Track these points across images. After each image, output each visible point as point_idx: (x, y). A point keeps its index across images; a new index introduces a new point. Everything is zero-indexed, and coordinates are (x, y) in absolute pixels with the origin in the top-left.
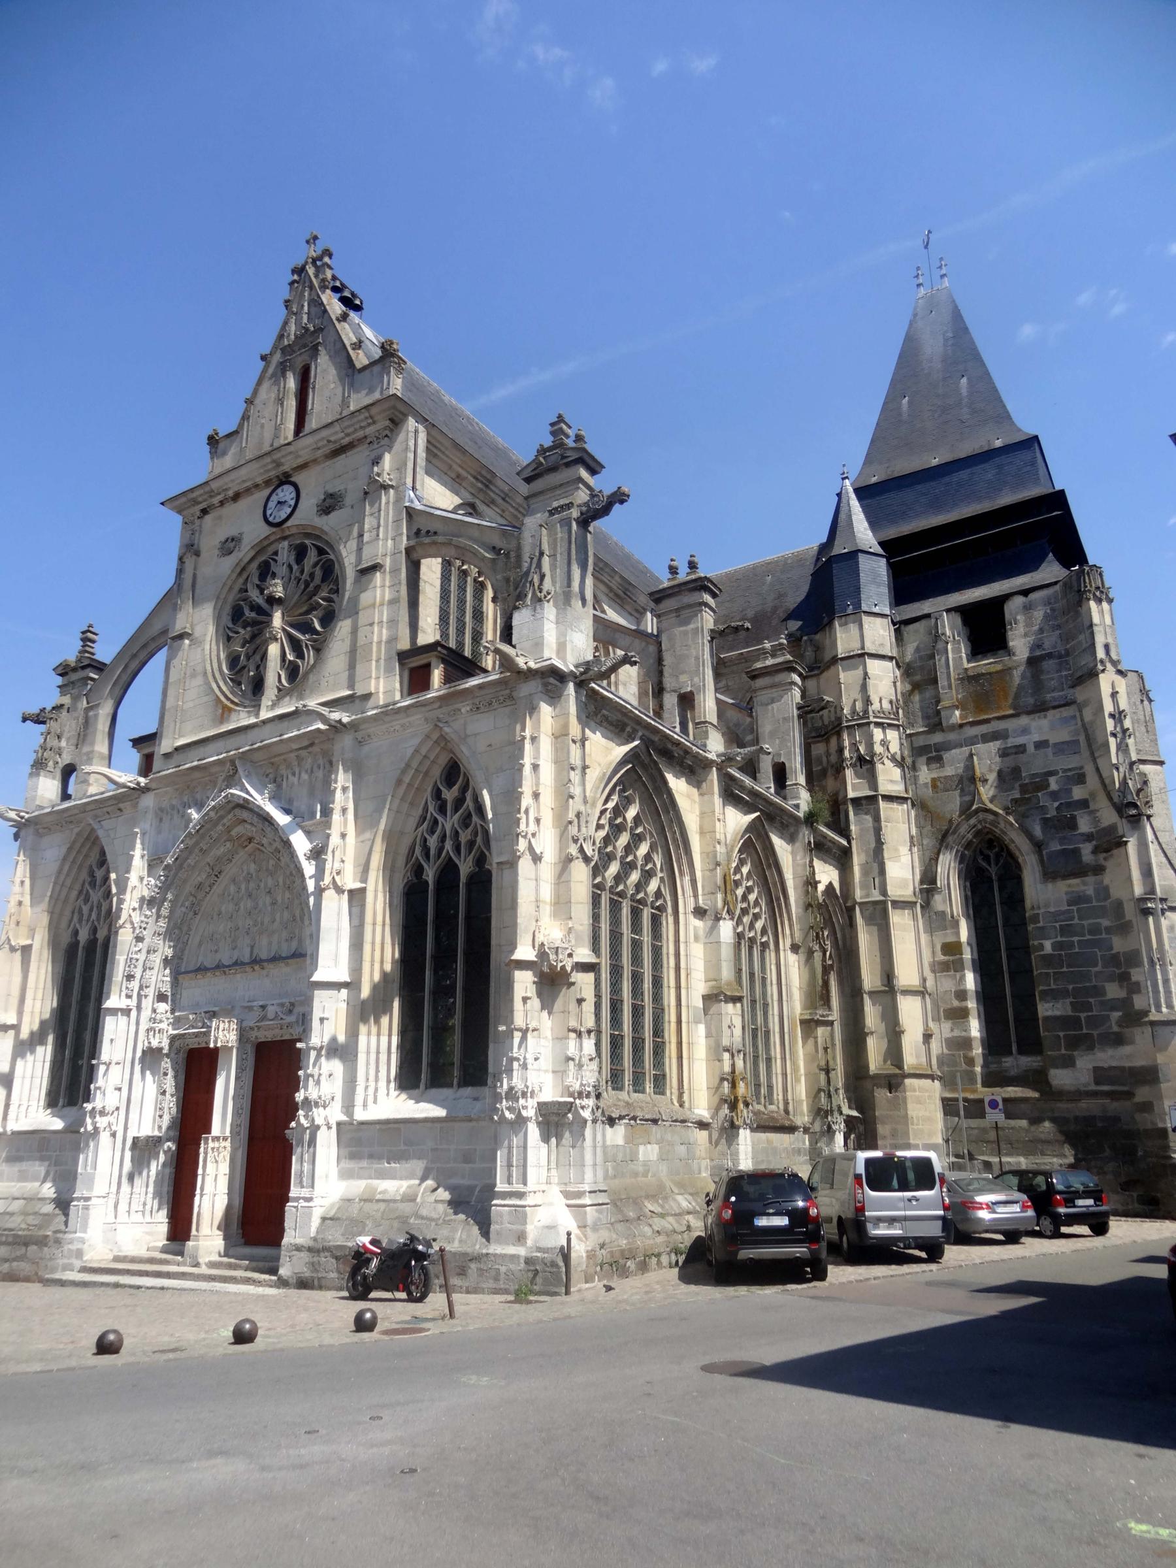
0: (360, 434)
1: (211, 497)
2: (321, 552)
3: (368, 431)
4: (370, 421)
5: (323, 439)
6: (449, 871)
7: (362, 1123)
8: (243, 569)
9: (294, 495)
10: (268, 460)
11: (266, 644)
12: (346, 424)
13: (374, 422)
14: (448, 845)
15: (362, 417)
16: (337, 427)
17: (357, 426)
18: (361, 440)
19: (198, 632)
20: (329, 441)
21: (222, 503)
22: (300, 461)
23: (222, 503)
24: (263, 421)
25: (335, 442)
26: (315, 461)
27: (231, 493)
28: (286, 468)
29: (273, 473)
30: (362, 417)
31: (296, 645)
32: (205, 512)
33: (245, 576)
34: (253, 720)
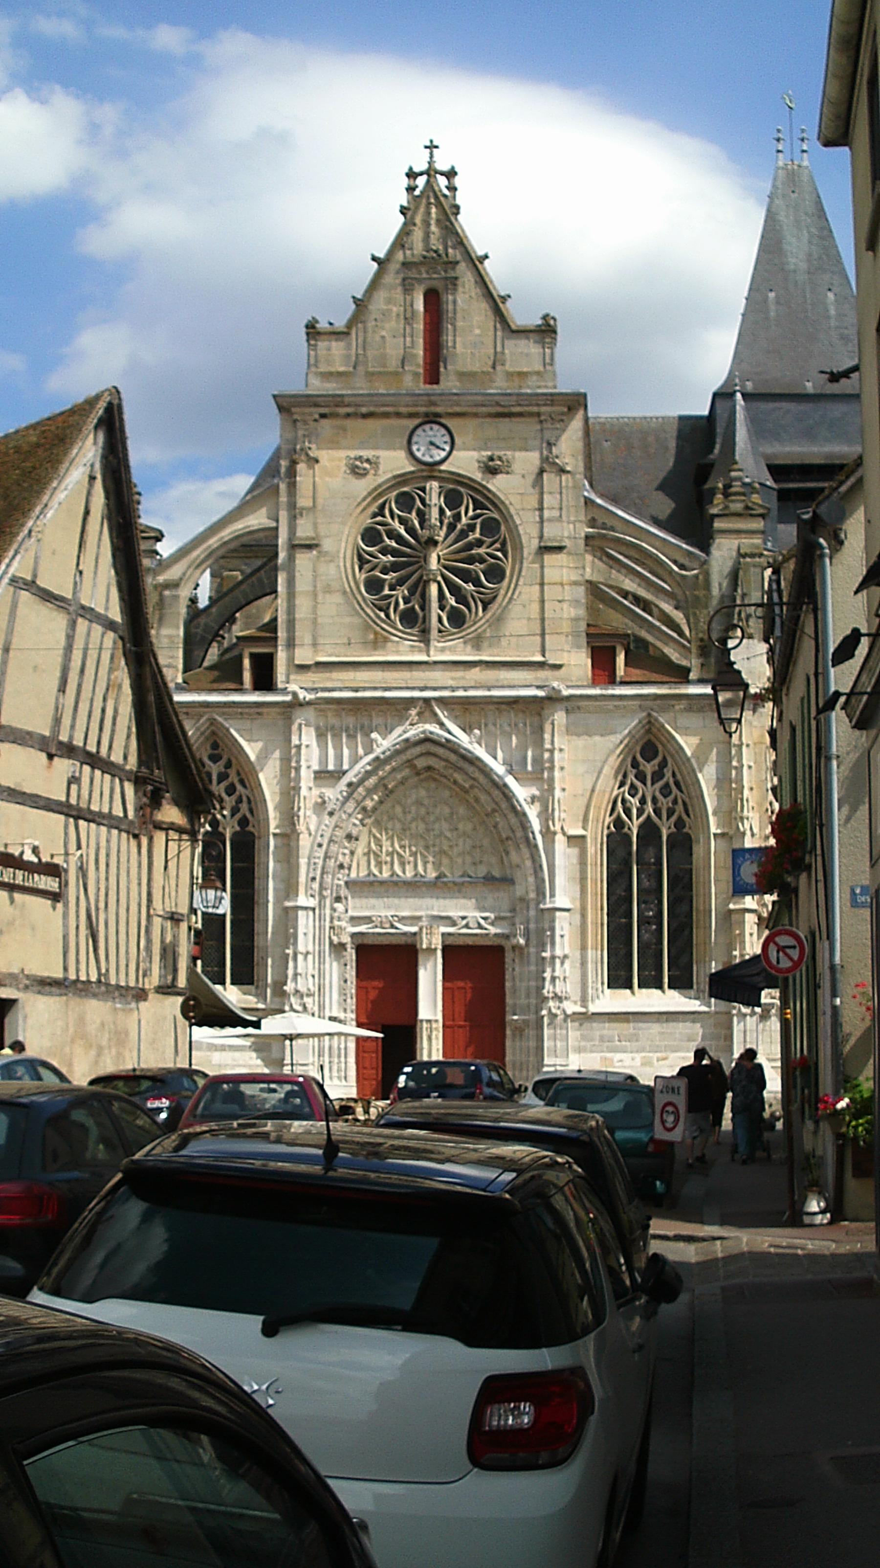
0: (535, 409)
1: (337, 406)
2: (477, 505)
3: (543, 409)
6: (649, 831)
7: (593, 1014)
8: (380, 495)
9: (447, 438)
10: (425, 398)
11: (427, 583)
13: (552, 405)
14: (649, 808)
16: (515, 398)
18: (531, 415)
19: (327, 545)
20: (498, 404)
21: (348, 415)
22: (458, 409)
23: (348, 415)
24: (384, 333)
26: (476, 415)
27: (364, 410)
28: (439, 410)
29: (423, 409)
31: (455, 590)
32: (323, 416)
33: (381, 501)
34: (423, 658)
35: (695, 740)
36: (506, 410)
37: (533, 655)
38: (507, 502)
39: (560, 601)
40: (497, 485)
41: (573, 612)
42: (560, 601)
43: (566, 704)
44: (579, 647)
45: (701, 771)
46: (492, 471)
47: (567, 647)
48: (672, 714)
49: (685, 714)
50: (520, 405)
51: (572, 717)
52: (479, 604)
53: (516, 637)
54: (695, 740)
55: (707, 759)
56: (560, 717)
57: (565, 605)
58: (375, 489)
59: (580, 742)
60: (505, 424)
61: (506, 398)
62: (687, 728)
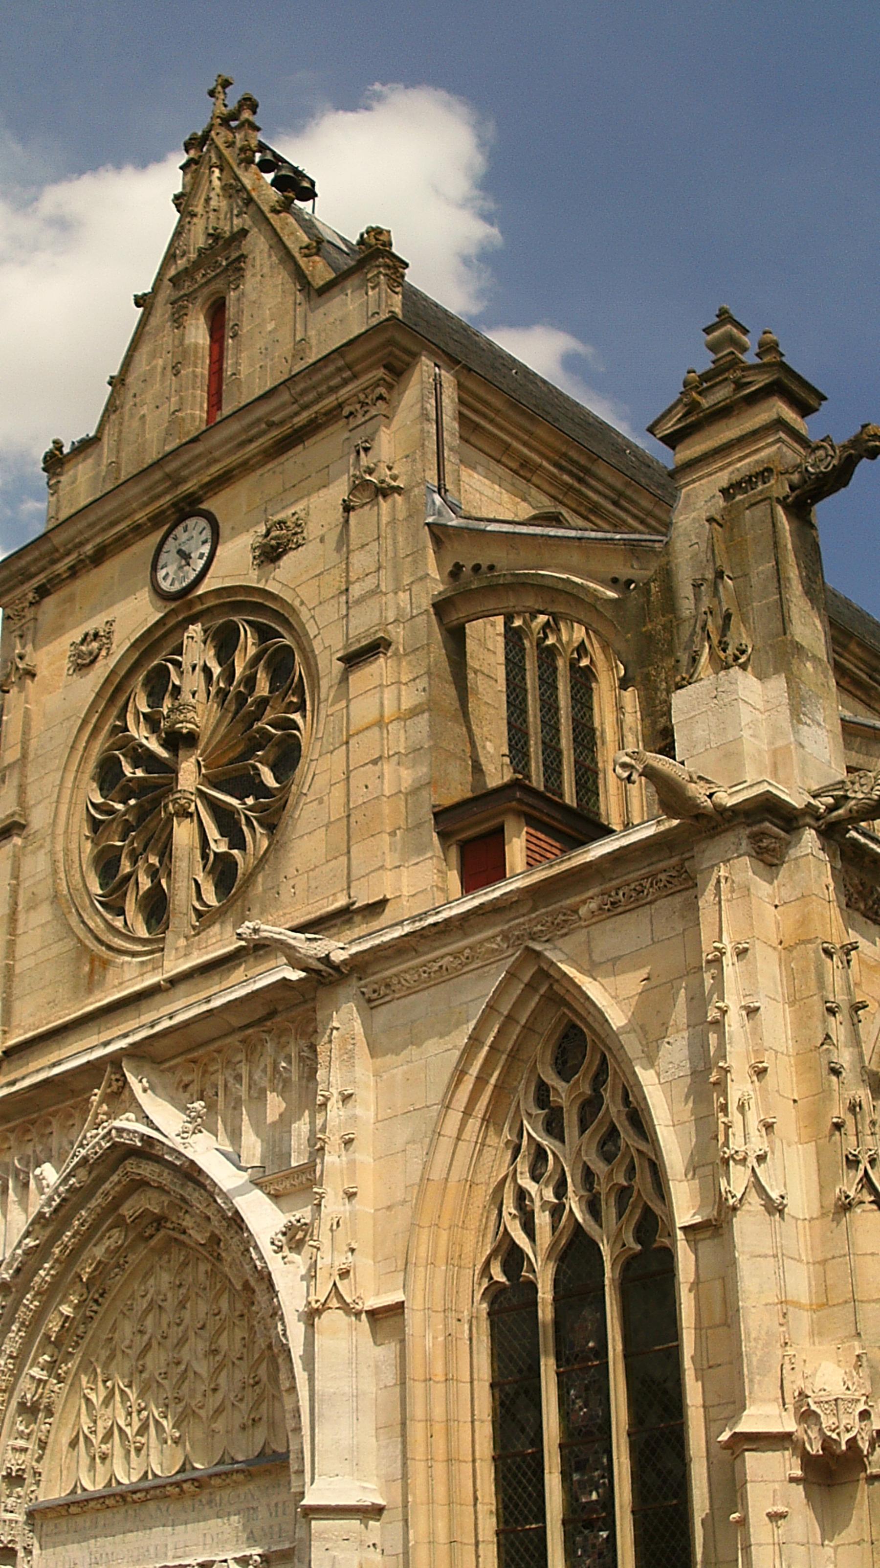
0: (329, 401)
3: (344, 393)
4: (347, 374)
5: (259, 421)
12: (302, 386)
13: (355, 376)
15: (331, 368)
16: (285, 397)
17: (323, 388)
20: (271, 425)
25: (282, 422)
30: (331, 368)
35: (632, 983)
36: (286, 429)
37: (335, 900)
38: (297, 603)
39: (375, 762)
40: (284, 579)
41: (407, 777)
42: (375, 762)
43: (353, 986)
44: (421, 849)
45: (651, 1061)
46: (270, 554)
47: (391, 860)
48: (580, 936)
49: (609, 925)
50: (305, 407)
51: (383, 1015)
52: (259, 830)
53: (307, 872)
54: (632, 983)
55: (665, 1025)
56: (345, 1019)
57: (388, 768)
58: (107, 680)
59: (398, 1066)
60: (297, 456)
61: (274, 403)
62: (614, 960)
